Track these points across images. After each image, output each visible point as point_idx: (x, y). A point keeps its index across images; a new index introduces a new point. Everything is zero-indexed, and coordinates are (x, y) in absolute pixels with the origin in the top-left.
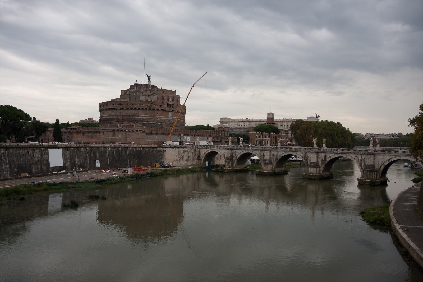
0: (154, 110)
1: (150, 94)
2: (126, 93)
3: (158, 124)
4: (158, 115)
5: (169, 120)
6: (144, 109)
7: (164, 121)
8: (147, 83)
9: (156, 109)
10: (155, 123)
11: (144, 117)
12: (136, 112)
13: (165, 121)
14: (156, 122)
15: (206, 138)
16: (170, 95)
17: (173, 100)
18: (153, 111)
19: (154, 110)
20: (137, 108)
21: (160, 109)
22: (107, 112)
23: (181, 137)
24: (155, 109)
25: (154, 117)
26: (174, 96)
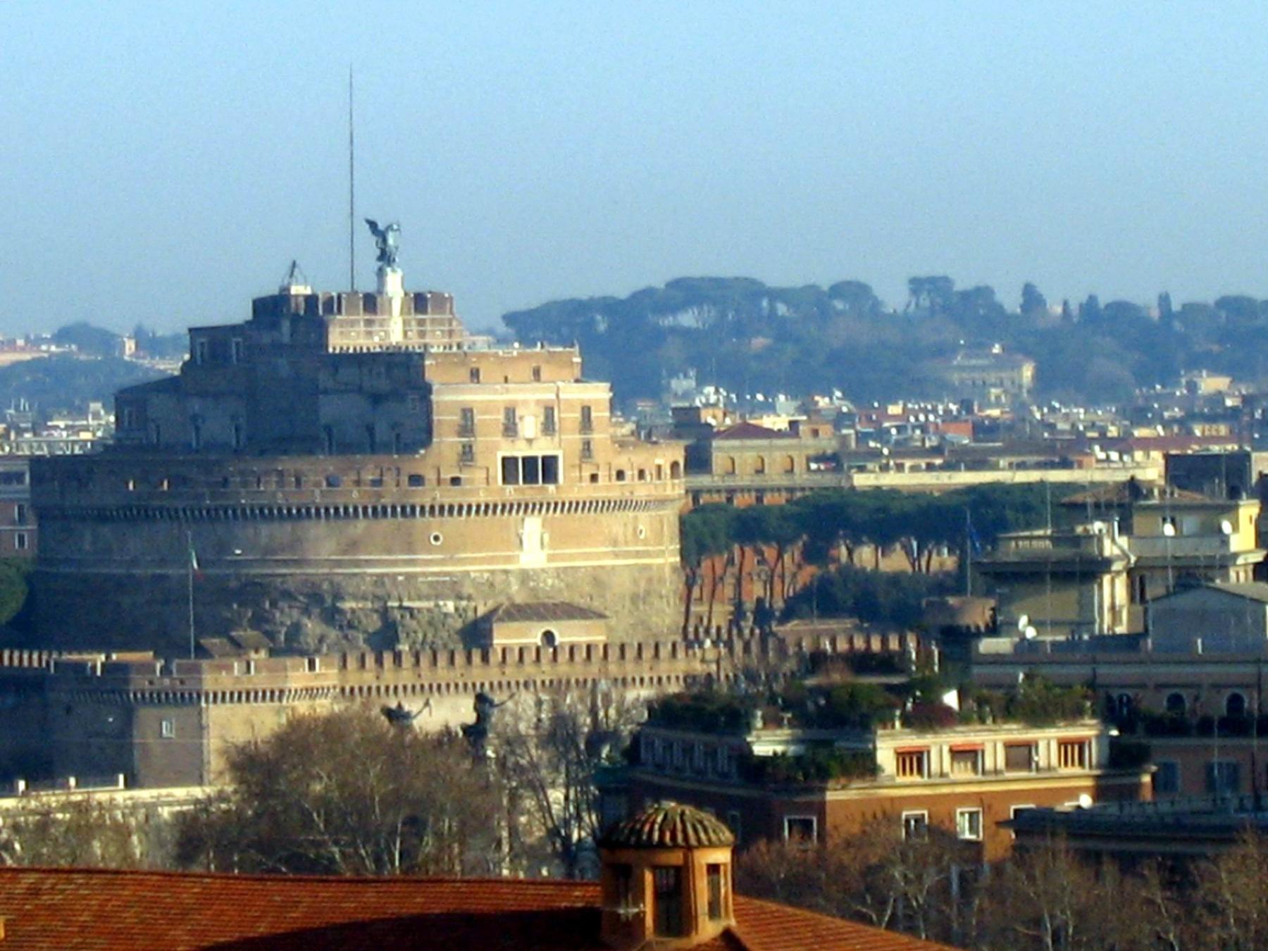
1: (383, 385)
2: (227, 358)
3: (445, 610)
4: (439, 550)
5: (525, 576)
6: (337, 509)
8: (366, 284)
9: (422, 508)
11: (339, 563)
12: (282, 531)
14: (428, 598)
18: (400, 519)
19: (409, 511)
20: (289, 511)
21: (451, 508)
22: (88, 536)
24: (413, 508)
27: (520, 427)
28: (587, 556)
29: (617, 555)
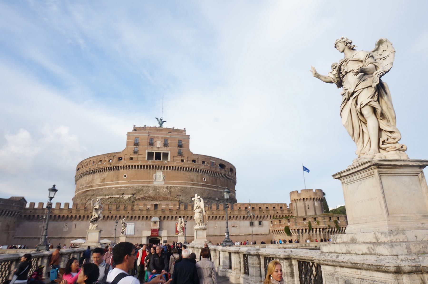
0: (117, 168)
3: (125, 198)
5: (155, 188)
7: (139, 191)
9: (121, 166)
10: (118, 196)
11: (100, 185)
13: (142, 190)
15: (247, 223)
16: (156, 136)
17: (166, 145)
19: (117, 168)
21: (129, 166)
23: (152, 223)
24: (118, 167)
25: (118, 184)
26: (170, 137)
27: (155, 144)
28: (181, 184)
29: (193, 185)
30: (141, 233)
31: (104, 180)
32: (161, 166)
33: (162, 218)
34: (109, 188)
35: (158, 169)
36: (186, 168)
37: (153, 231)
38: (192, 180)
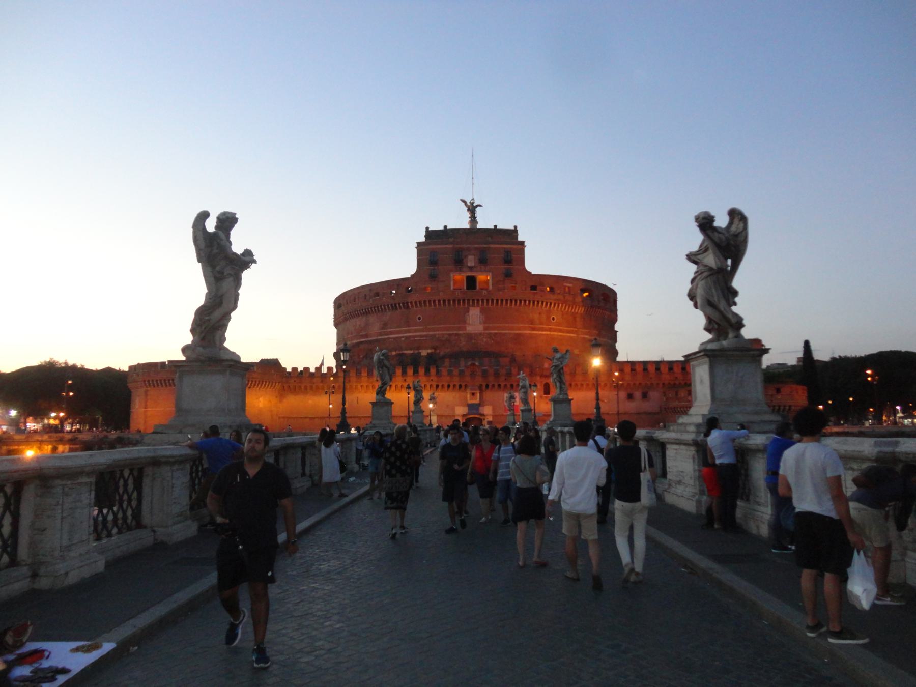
0: (406, 306)
5: (470, 337)
11: (381, 334)
15: (623, 395)
16: (465, 246)
17: (483, 261)
19: (406, 306)
25: (409, 331)
30: (453, 409)
31: (385, 325)
32: (478, 300)
33: (484, 388)
34: (394, 339)
35: (473, 305)
36: (520, 301)
37: (470, 406)
38: (532, 322)
